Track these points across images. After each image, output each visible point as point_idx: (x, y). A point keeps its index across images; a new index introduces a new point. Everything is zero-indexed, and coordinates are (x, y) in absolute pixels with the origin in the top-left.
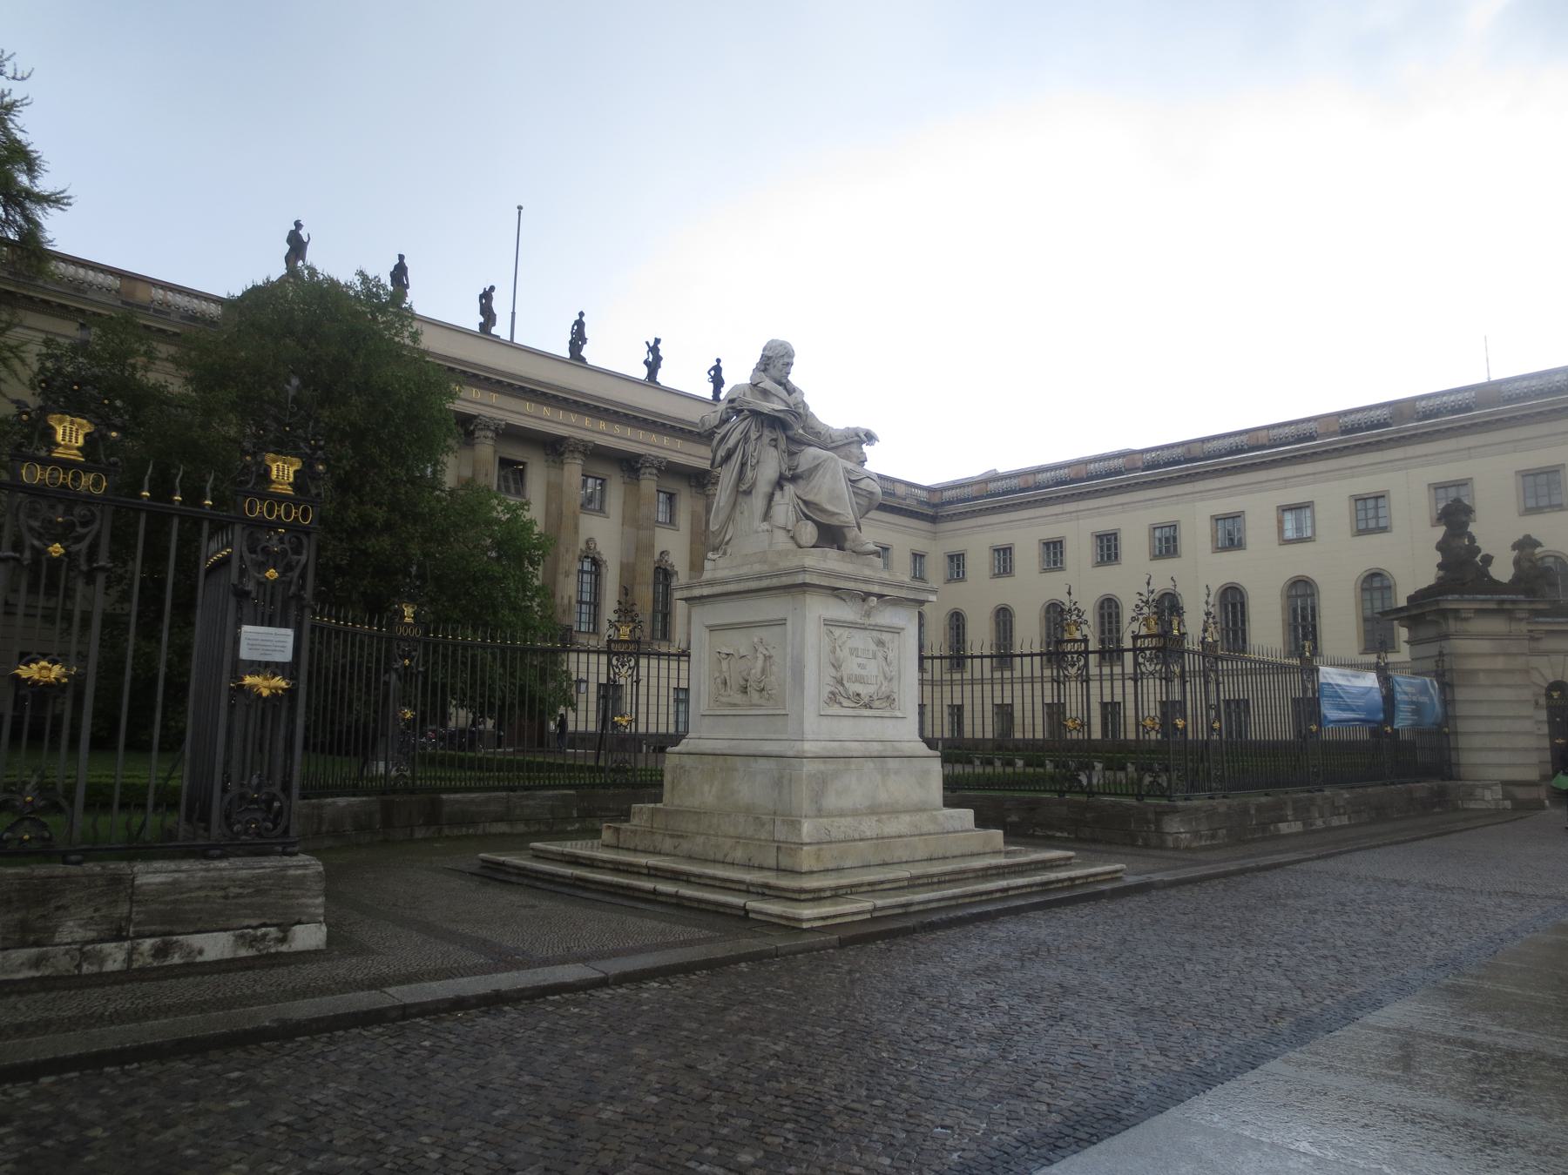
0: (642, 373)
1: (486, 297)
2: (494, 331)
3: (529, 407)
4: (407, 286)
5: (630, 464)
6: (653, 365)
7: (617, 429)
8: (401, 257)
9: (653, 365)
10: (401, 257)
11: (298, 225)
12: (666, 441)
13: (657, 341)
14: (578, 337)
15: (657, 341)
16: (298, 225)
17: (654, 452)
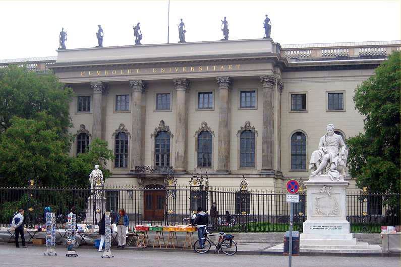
0: (221, 36)
1: (137, 29)
2: (142, 42)
3: (154, 71)
4: (102, 37)
5: (214, 82)
6: (226, 31)
7: (201, 69)
8: (99, 26)
9: (226, 31)
10: (99, 26)
11: (63, 29)
12: (230, 67)
13: (225, 18)
14: (182, 33)
15: (225, 18)
16: (63, 29)
17: (222, 74)
